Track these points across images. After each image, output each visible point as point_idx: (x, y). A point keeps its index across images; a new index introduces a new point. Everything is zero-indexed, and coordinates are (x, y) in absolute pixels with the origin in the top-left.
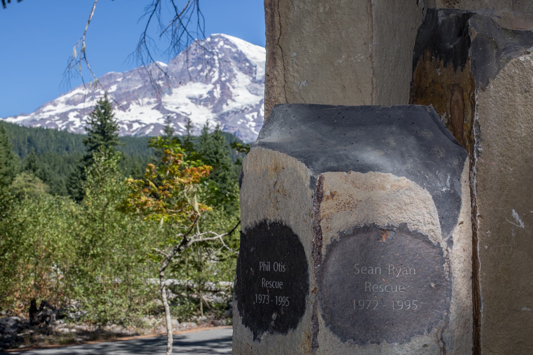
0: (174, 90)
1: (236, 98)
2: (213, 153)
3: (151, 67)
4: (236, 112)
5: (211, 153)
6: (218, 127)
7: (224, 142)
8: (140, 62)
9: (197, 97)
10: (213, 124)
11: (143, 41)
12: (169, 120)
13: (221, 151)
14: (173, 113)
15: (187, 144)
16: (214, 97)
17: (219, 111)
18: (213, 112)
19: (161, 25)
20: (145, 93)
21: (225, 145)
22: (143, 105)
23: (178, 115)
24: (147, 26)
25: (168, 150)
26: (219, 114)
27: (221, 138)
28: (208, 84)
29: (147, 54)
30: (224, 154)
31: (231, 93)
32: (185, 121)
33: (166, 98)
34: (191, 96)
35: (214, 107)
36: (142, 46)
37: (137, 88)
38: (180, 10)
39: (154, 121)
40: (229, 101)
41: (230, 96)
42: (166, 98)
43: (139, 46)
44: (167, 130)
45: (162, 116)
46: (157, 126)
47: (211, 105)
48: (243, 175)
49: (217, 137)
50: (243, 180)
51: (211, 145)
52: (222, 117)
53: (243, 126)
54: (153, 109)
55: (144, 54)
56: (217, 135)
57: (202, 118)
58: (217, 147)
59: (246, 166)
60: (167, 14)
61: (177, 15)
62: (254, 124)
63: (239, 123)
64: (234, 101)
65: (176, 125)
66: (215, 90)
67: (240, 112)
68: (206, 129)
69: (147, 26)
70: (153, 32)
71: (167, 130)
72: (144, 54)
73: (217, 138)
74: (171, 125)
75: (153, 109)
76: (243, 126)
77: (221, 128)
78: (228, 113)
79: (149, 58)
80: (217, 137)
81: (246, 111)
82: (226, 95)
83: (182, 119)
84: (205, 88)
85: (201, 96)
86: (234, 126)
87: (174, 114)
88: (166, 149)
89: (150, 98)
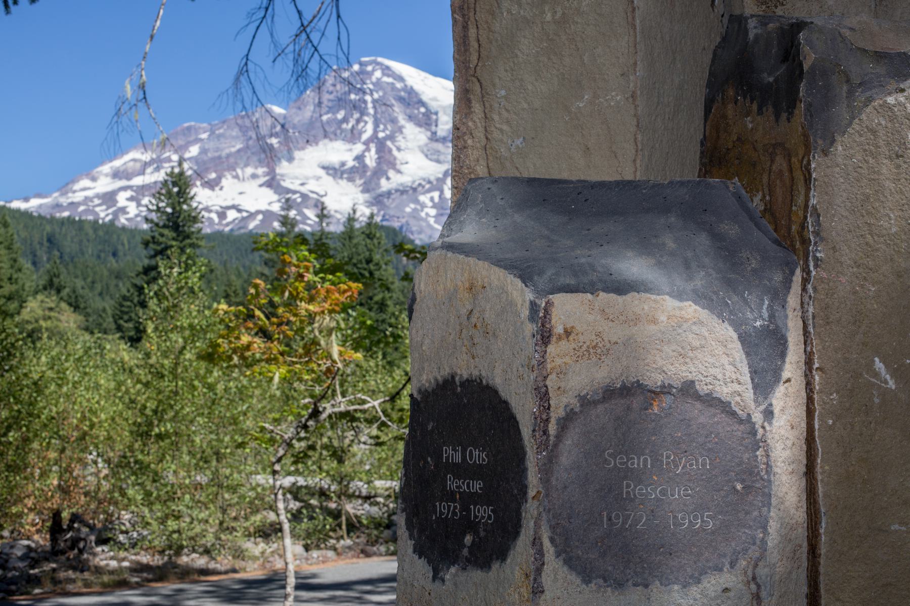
0: (297, 154)
1: (403, 168)
2: (364, 261)
3: (257, 115)
4: (402, 191)
5: (361, 262)
6: (372, 216)
7: (382, 242)
8: (239, 105)
9: (337, 166)
10: (364, 212)
11: (244, 70)
12: (288, 205)
13: (377, 257)
14: (295, 192)
15: (319, 245)
16: (365, 166)
17: (374, 189)
18: (363, 192)
19: (274, 43)
20: (248, 158)
21: (384, 248)
22: (244, 180)
23: (304, 196)
24: (251, 45)
25: (286, 257)
26: (373, 194)
27: (378, 235)
28: (354, 144)
29: (250, 92)
30: (382, 263)
31: (395, 159)
32: (316, 206)
33: (283, 168)
34: (327, 164)
35: (365, 183)
36: (243, 79)
37: (233, 150)
38: (307, 16)
39: (264, 207)
40: (391, 173)
41: (393, 165)
42: (283, 168)
43: (237, 79)
44: (285, 221)
45: (276, 197)
46: (268, 215)
47: (360, 179)
48: (415, 300)
49: (371, 233)
50: (415, 307)
51: (360, 248)
52: (378, 200)
53: (415, 215)
54: (261, 186)
55: (246, 92)
56: (371, 231)
57: (345, 201)
58: (370, 250)
59: (420, 284)
60: (285, 24)
61: (302, 25)
62: (433, 212)
63: (408, 210)
64: (399, 172)
65: (300, 213)
66: (367, 154)
67: (410, 192)
68: (351, 220)
69: (251, 45)
70: (262, 54)
71: (285, 221)
72: (246, 92)
73: (370, 236)
74: (292, 213)
75: (261, 186)
76: (415, 215)
77: (378, 219)
78: (389, 193)
79: (255, 99)
80: (371, 233)
81: (420, 189)
82: (386, 162)
83: (312, 202)
84: (351, 150)
85: (343, 164)
86: (400, 216)
87: (298, 195)
88: (284, 254)
89: (256, 168)
